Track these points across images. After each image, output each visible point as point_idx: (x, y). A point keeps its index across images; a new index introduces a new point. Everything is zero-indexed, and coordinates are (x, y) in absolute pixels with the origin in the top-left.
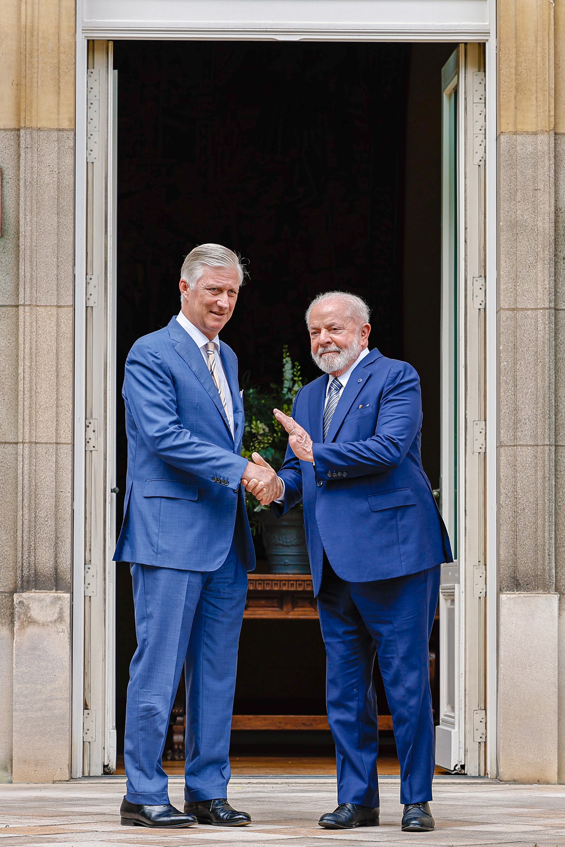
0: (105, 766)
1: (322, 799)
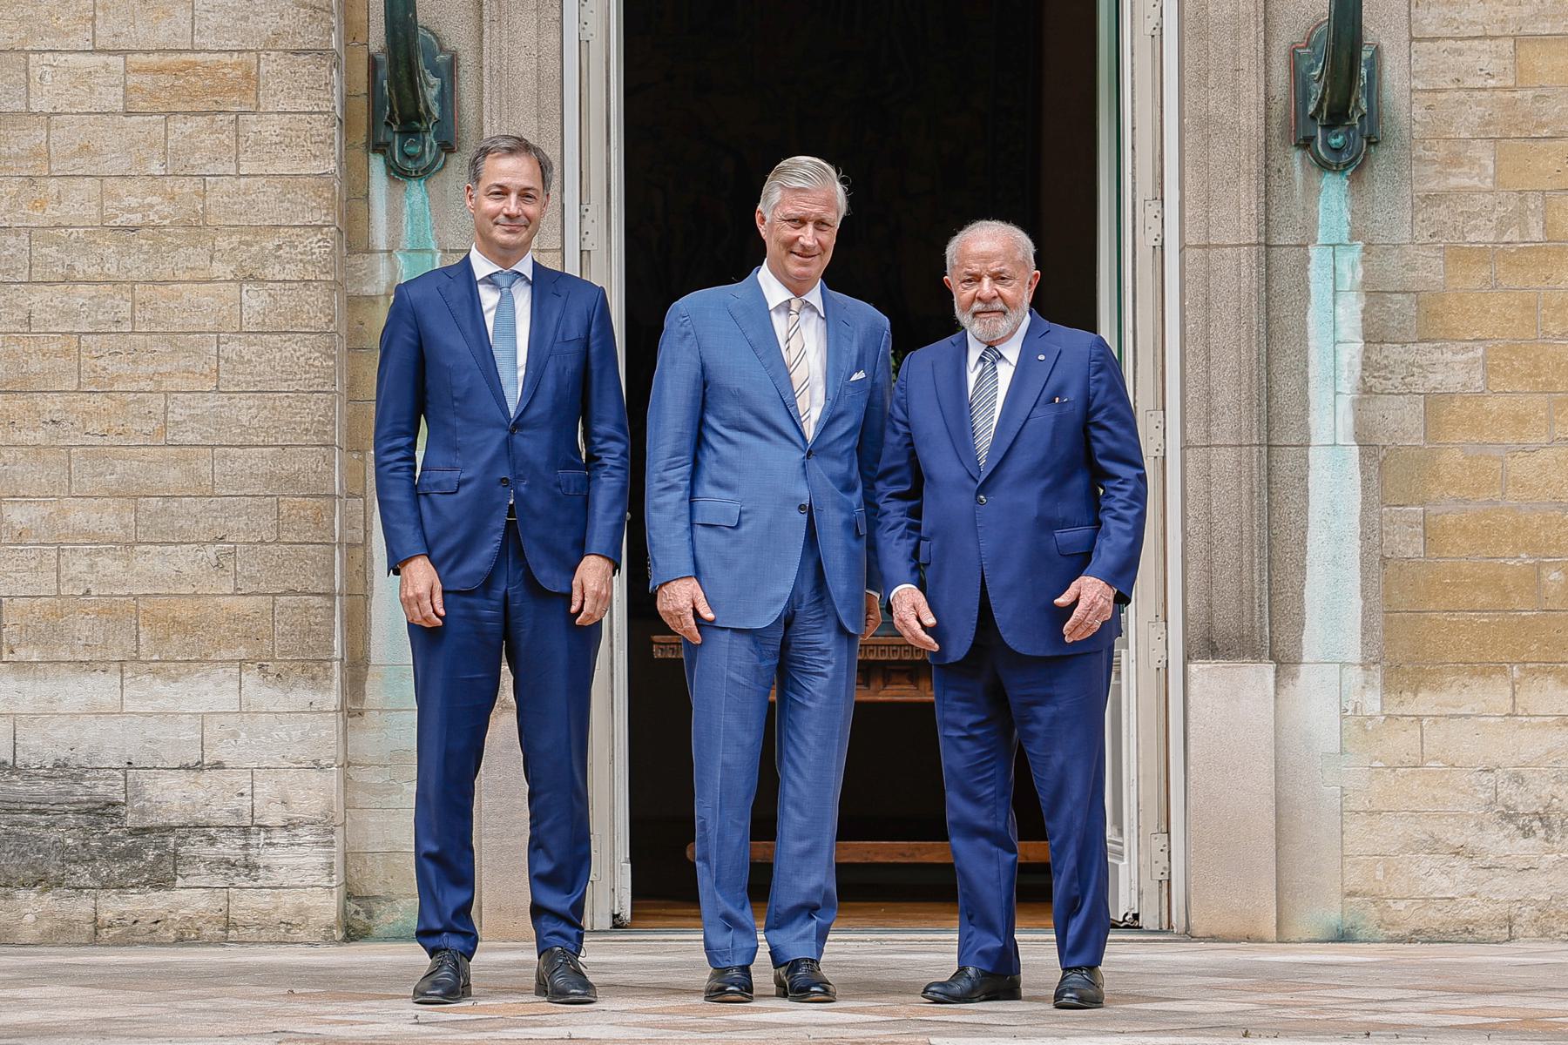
0: (615, 916)
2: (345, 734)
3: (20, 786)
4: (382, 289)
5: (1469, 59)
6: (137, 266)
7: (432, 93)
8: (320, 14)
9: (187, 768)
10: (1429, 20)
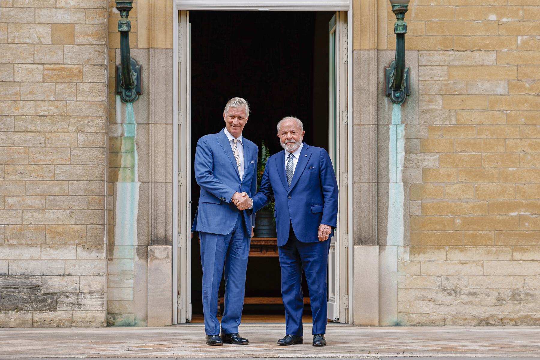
0: (187, 319)
1: (279, 333)
2: (107, 266)
3: (10, 281)
4: (119, 135)
5: (435, 72)
6: (47, 127)
7: (134, 77)
8: (101, 54)
9: (60, 275)
10: (424, 60)
